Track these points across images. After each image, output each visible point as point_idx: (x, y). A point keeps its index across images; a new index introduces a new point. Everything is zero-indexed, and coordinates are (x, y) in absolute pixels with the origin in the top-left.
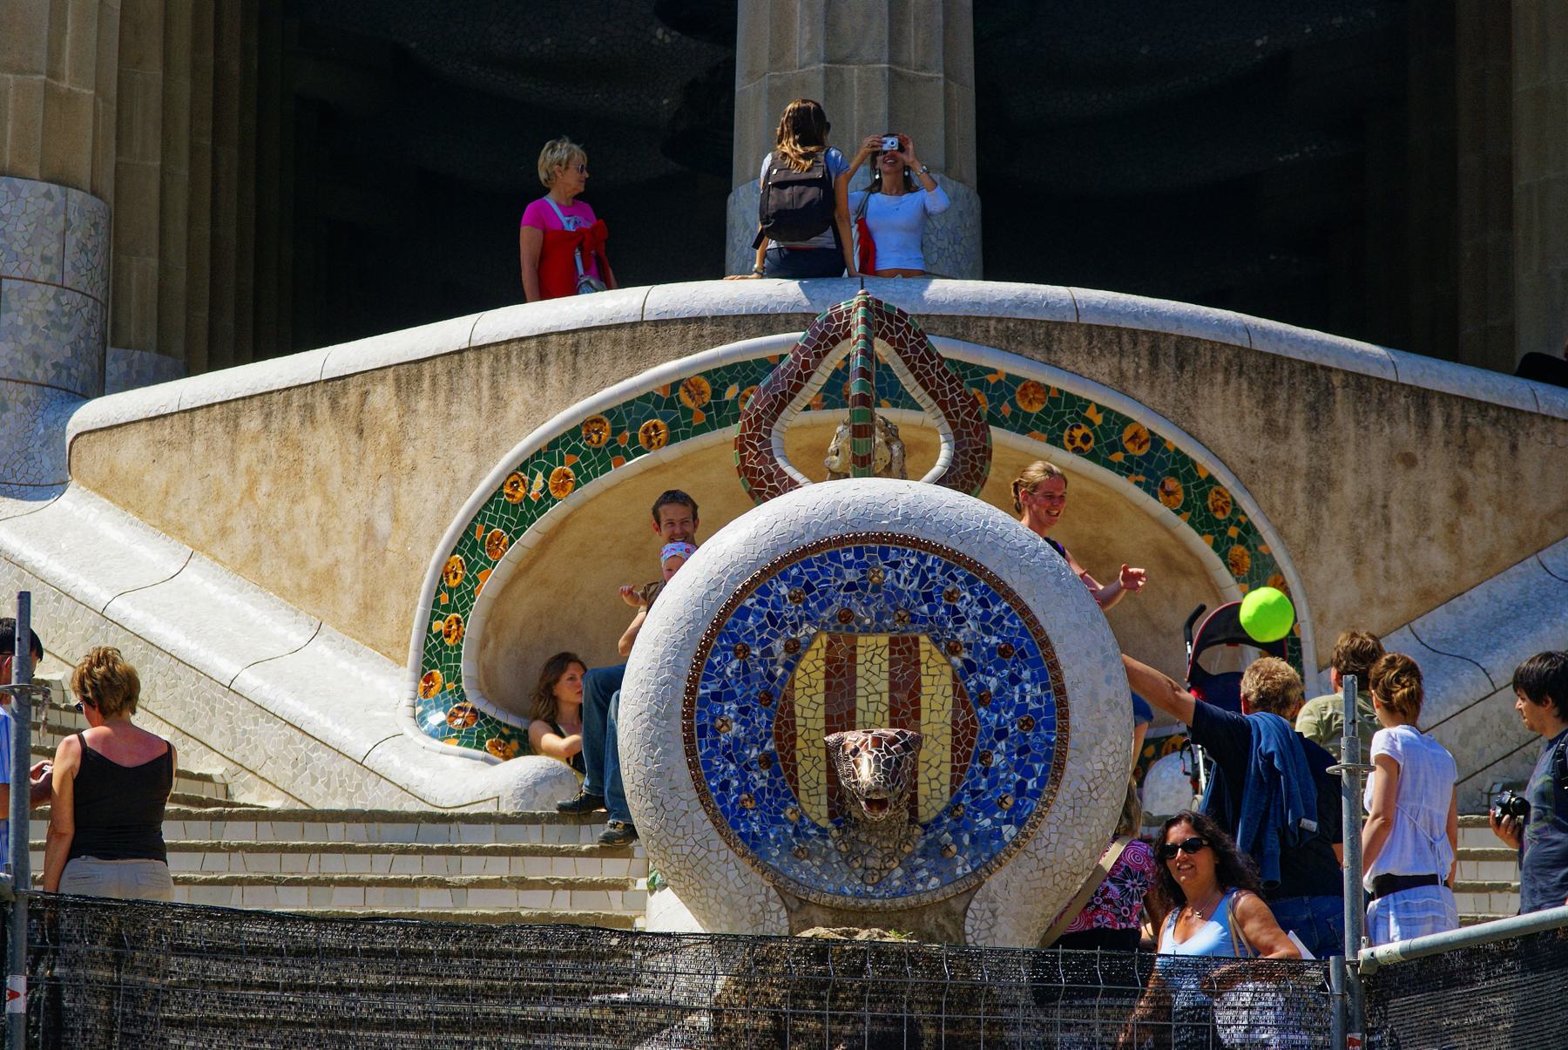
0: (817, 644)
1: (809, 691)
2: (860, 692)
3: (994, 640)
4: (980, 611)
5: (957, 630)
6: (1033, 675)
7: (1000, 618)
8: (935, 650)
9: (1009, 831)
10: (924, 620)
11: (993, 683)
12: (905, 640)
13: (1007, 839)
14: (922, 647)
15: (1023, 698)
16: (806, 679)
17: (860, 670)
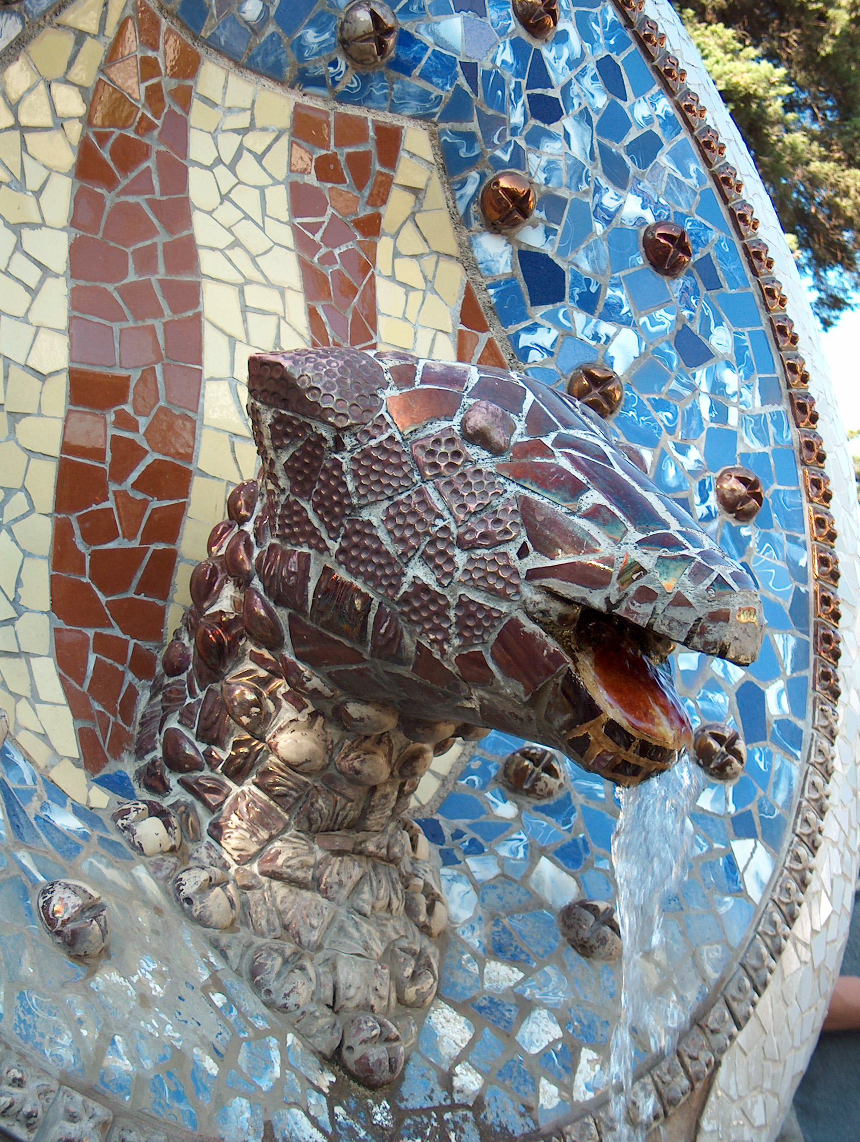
2: (208, 263)
3: (632, 208)
4: (601, 101)
5: (535, 139)
6: (739, 349)
8: (437, 194)
9: (755, 861)
10: (444, 65)
11: (623, 350)
12: (351, 130)
13: (754, 892)
15: (720, 411)
17: (200, 187)
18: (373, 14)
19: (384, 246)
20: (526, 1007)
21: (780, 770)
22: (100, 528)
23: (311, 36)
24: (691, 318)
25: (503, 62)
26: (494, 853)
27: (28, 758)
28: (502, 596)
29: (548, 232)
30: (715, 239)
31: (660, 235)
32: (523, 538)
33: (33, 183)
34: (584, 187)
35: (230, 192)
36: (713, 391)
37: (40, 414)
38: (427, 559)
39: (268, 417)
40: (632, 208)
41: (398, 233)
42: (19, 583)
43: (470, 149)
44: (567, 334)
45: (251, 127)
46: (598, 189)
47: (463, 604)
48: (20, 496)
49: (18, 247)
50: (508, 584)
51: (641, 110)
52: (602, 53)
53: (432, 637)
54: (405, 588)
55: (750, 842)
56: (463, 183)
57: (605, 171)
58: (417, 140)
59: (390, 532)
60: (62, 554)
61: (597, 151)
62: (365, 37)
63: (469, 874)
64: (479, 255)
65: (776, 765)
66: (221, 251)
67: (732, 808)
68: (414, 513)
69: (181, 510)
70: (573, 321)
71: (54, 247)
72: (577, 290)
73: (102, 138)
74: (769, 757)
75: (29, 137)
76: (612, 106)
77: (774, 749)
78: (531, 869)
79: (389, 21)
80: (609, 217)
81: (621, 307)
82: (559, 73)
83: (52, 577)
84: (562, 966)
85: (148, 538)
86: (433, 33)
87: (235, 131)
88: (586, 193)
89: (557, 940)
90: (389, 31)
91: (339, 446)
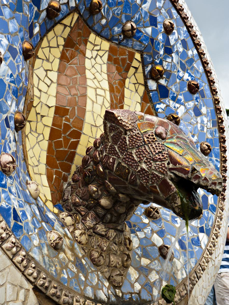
0: (67, 21)
1: (47, 65)
2: (89, 83)
5: (165, 58)
6: (208, 113)
7: (191, 61)
8: (140, 69)
10: (147, 38)
11: (181, 112)
14: (135, 64)
16: (46, 50)
18: (131, 25)
19: (127, 81)
20: (151, 270)
21: (210, 217)
22: (59, 144)
23: (116, 29)
24: (198, 104)
25: (160, 39)
26: (143, 231)
27: (41, 200)
28: (162, 174)
29: (166, 80)
30: (204, 86)
31: (192, 84)
32: (169, 160)
33: (51, 60)
34: (175, 70)
35: (94, 65)
36: (201, 123)
37: (48, 116)
38: (145, 162)
39: (109, 125)
40: (186, 76)
41: (131, 77)
42: (39, 157)
43: (150, 59)
44: (168, 106)
45: (100, 50)
46: (178, 71)
47: (153, 174)
48: (42, 135)
49: (46, 76)
50: (164, 170)
51: (190, 53)
52: (182, 38)
53: (144, 181)
54: (139, 169)
55: (203, 234)
56: (147, 67)
57: (181, 67)
58: (138, 56)
59: (137, 155)
60: (49, 150)
61: (179, 62)
62: (128, 31)
63: (137, 235)
64: (149, 84)
65: (210, 216)
66: (92, 80)
67: (199, 225)
68: (143, 151)
69: (78, 141)
70: (169, 102)
71: (54, 76)
72: (171, 95)
73: (67, 50)
74: (208, 213)
75: (51, 49)
76: (184, 51)
77: (209, 211)
78: (152, 236)
79: (135, 27)
80: (181, 78)
81: (181, 100)
82: (172, 42)
83: (47, 155)
84: (159, 261)
85: (70, 148)
86: (145, 31)
87: (97, 50)
88: (175, 72)
89: (158, 254)
90: (135, 29)
91: (126, 134)
